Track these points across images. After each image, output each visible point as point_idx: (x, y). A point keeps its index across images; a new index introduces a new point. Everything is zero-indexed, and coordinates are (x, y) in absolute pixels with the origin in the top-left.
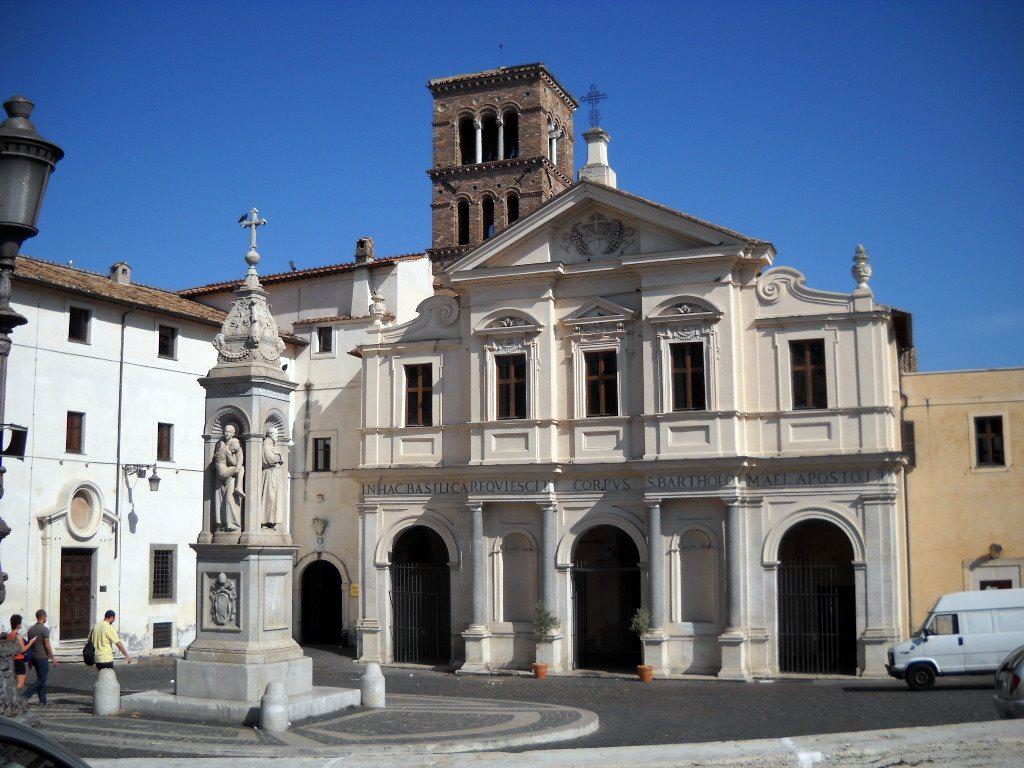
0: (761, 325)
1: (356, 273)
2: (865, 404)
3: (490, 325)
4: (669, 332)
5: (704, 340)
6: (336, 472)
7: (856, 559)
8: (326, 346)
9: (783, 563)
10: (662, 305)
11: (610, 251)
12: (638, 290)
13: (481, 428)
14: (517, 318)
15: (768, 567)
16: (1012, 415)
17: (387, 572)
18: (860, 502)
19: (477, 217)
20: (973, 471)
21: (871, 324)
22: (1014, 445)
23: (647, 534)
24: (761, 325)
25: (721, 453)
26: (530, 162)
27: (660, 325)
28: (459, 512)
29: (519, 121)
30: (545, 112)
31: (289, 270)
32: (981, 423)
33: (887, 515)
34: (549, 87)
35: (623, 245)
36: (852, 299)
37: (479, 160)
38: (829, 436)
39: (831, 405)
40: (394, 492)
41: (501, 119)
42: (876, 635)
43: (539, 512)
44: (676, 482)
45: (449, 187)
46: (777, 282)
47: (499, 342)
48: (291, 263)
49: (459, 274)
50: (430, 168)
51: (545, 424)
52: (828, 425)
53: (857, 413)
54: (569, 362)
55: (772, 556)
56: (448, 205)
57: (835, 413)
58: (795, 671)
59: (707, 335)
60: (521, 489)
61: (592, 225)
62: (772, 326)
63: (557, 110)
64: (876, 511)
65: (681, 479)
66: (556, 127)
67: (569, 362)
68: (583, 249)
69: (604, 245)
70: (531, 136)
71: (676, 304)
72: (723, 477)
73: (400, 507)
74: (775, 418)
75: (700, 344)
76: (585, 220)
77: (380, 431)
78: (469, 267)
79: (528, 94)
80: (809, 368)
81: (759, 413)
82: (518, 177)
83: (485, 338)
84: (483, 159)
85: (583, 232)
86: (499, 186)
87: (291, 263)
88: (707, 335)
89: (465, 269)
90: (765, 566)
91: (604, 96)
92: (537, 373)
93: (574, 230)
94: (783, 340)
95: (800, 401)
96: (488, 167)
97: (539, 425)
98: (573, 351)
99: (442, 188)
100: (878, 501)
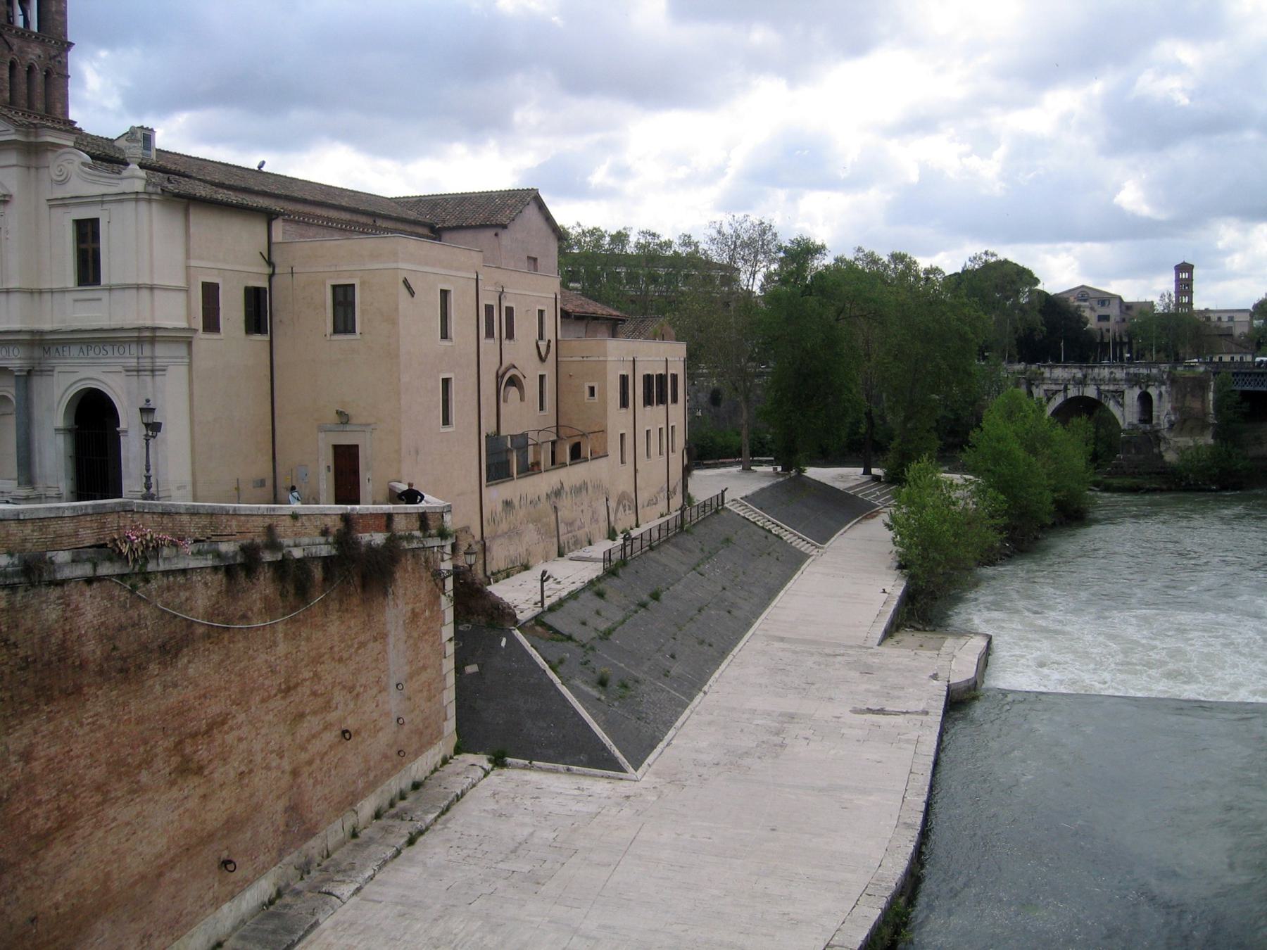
39: (103, 281)
90: (56, 430)
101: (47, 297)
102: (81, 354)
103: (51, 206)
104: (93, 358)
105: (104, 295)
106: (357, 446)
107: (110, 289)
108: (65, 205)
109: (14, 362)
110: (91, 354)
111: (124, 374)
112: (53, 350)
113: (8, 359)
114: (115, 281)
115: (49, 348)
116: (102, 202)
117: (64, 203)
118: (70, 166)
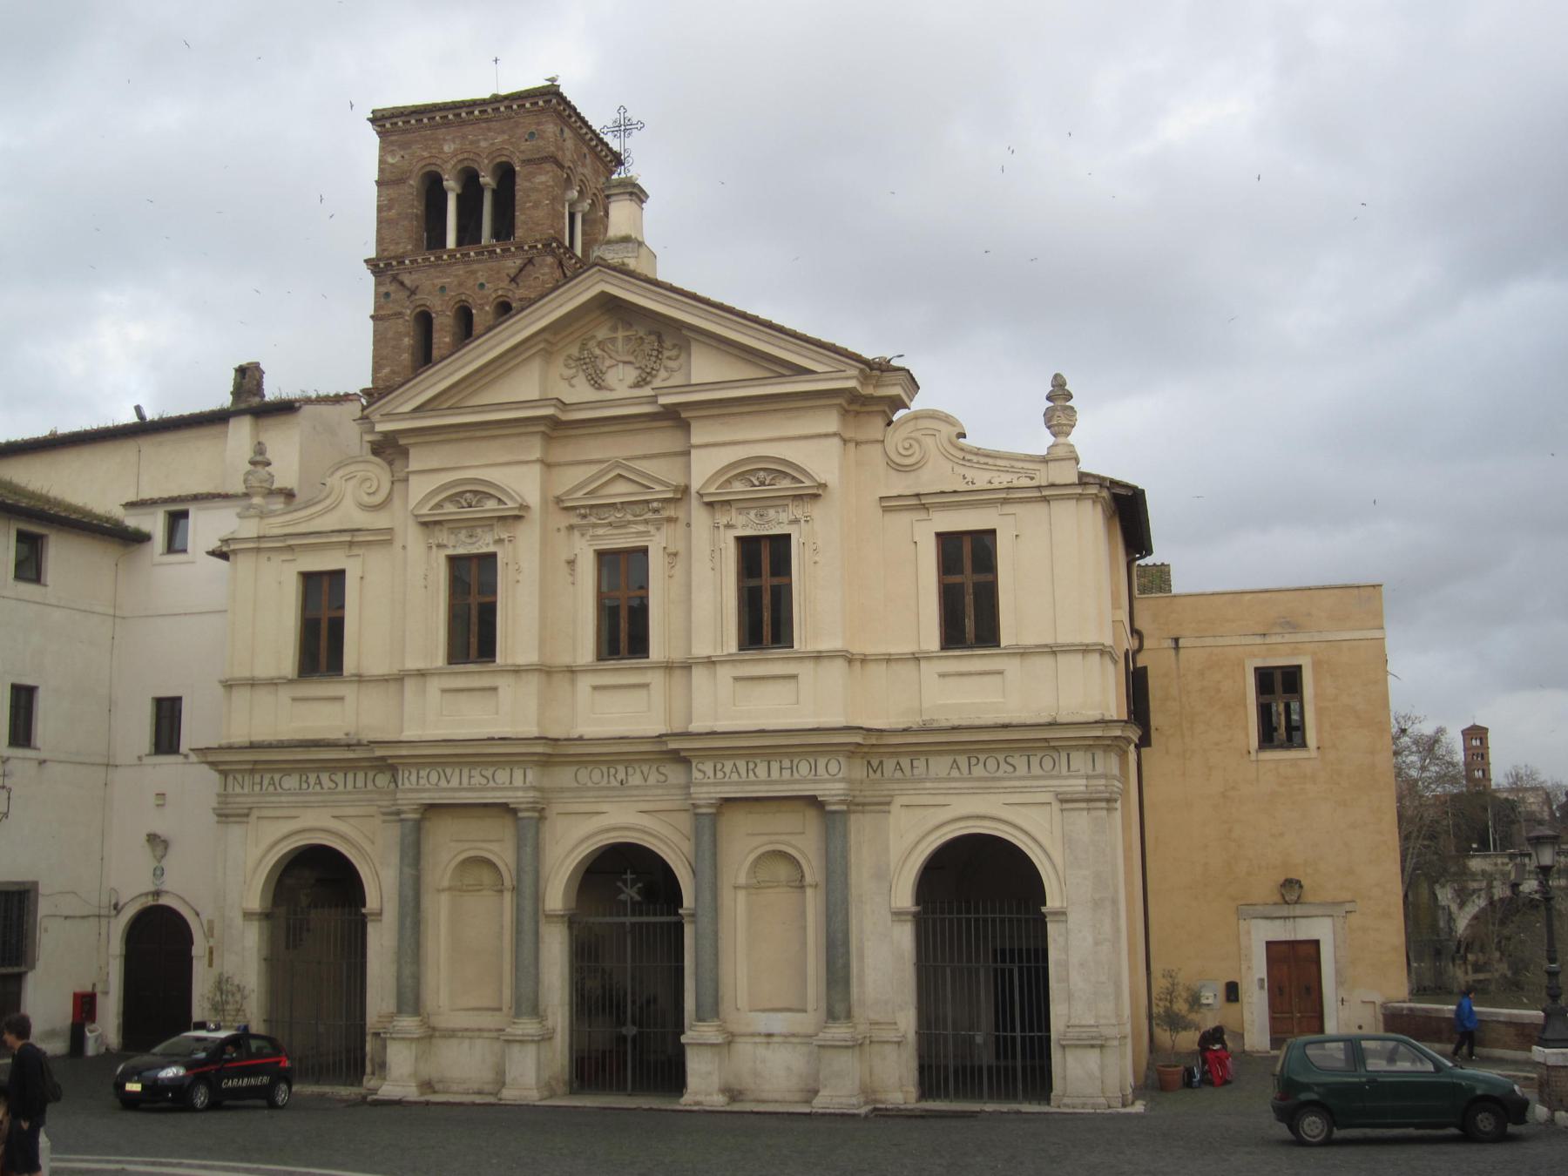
0: (889, 505)
1: (233, 423)
3: (439, 505)
8: (174, 544)
15: (898, 915)
16: (1317, 665)
19: (442, 338)
20: (1253, 756)
22: (1320, 712)
24: (889, 505)
28: (384, 822)
29: (518, 180)
30: (561, 166)
31: (132, 418)
32: (1265, 678)
34: (570, 127)
35: (663, 374)
37: (451, 241)
39: (1006, 638)
41: (487, 179)
42: (1084, 1035)
44: (743, 770)
48: (138, 409)
49: (389, 416)
50: (373, 255)
54: (571, 563)
55: (904, 896)
56: (399, 315)
58: (947, 1096)
60: (484, 781)
63: (584, 165)
65: (751, 766)
66: (581, 192)
69: (631, 374)
70: (536, 205)
71: (745, 471)
73: (285, 813)
78: (407, 408)
79: (532, 135)
80: (967, 578)
84: (460, 241)
85: (597, 352)
86: (482, 286)
87: (138, 409)
89: (401, 410)
91: (641, 125)
95: (953, 636)
99: (392, 288)
101: (875, 670)
102: (955, 773)
103: (886, 510)
104: (979, 779)
105: (1012, 666)
106: (1269, 944)
107: (1024, 653)
108: (924, 507)
109: (828, 786)
110: (978, 771)
111: (1056, 806)
112: (890, 764)
113: (815, 782)
114: (1030, 640)
115: (881, 763)
116: (1005, 501)
117: (920, 503)
118: (929, 441)
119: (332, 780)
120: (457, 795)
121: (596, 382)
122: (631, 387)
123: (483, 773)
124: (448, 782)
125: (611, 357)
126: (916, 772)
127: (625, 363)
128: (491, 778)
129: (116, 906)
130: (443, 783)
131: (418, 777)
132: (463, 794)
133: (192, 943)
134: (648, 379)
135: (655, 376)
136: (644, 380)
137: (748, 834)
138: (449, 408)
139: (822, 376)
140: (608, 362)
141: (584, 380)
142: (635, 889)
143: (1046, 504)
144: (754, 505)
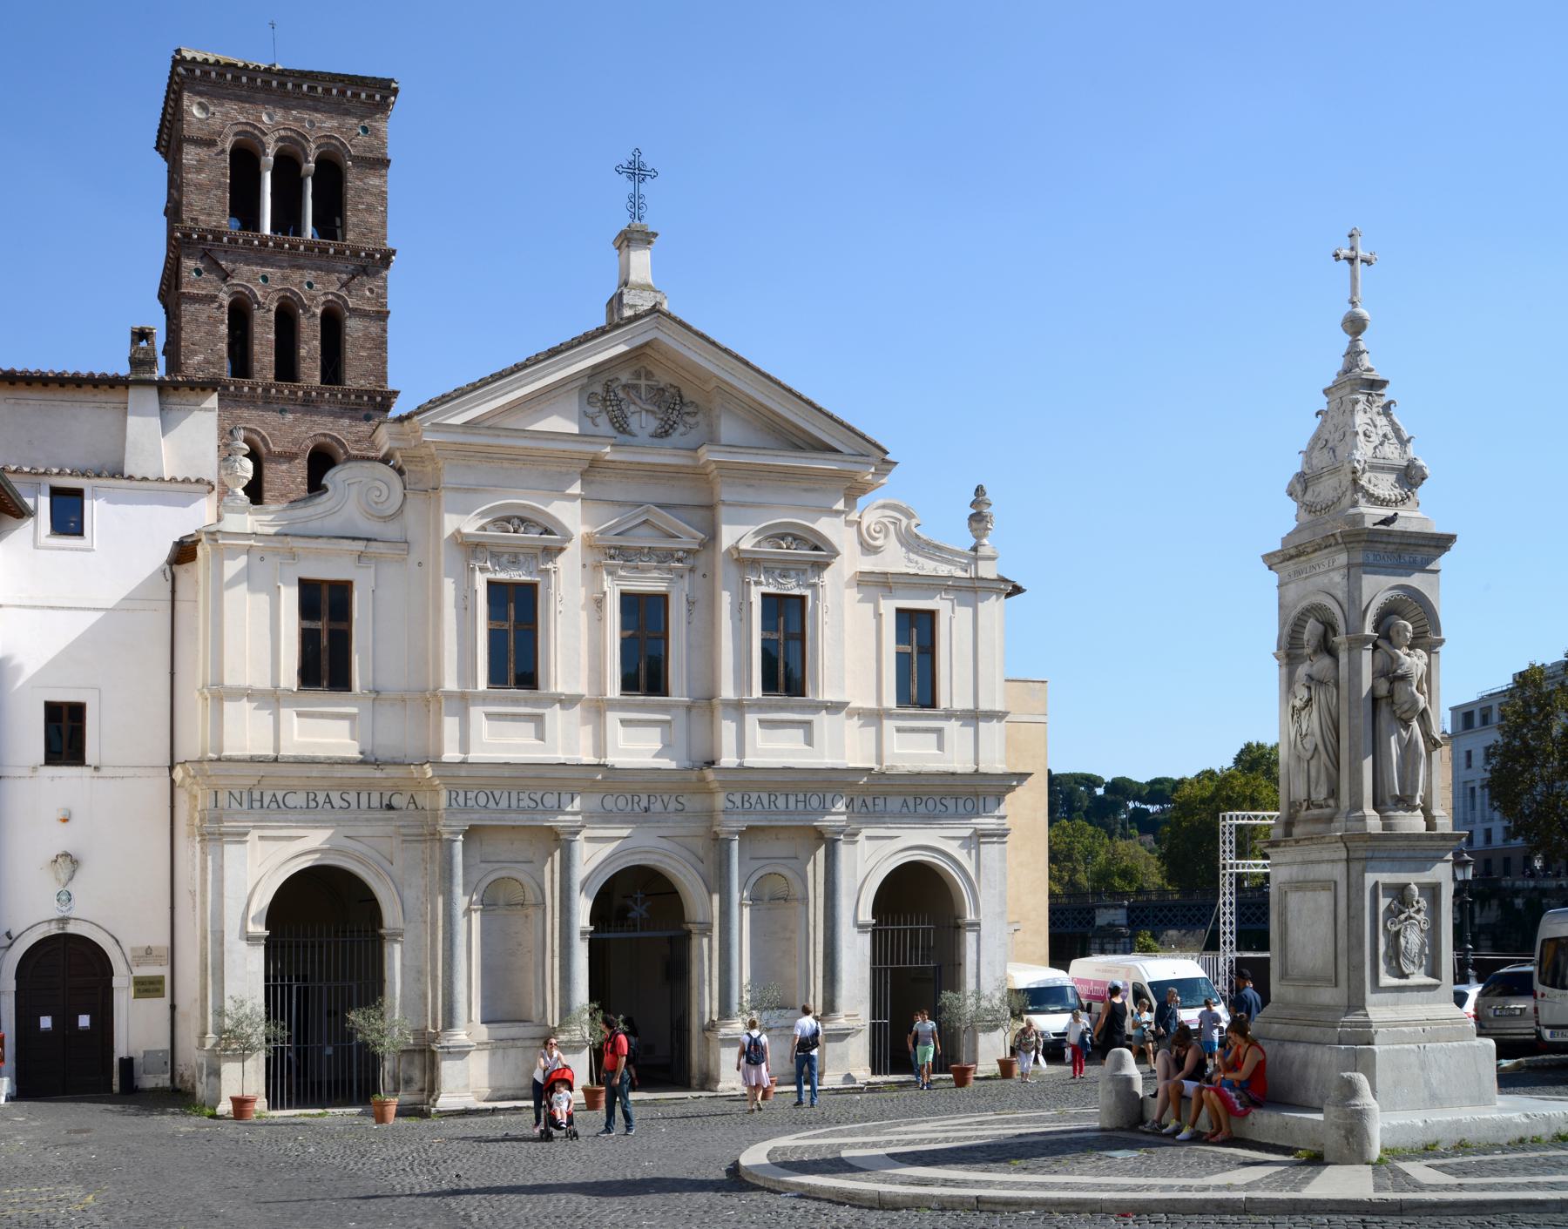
2: (984, 706)
4: (762, 576)
5: (808, 592)
6: (96, 768)
7: (968, 917)
9: (879, 923)
10: (757, 533)
11: (664, 433)
12: (711, 508)
13: (463, 701)
14: (524, 521)
17: (259, 952)
18: (980, 837)
21: (994, 597)
23: (720, 883)
25: (827, 761)
26: (370, 255)
27: (747, 562)
33: (1003, 859)
35: (681, 429)
36: (976, 559)
38: (940, 747)
40: (281, 806)
43: (560, 841)
45: (214, 266)
46: (885, 520)
47: (495, 556)
51: (567, 702)
52: (939, 731)
53: (974, 717)
57: (950, 715)
59: (814, 586)
60: (533, 805)
61: (636, 387)
62: (877, 584)
64: (989, 851)
67: (599, 603)
68: (621, 426)
69: (652, 424)
72: (829, 797)
74: (874, 717)
75: (802, 598)
76: (625, 377)
77: (250, 694)
78: (458, 420)
81: (859, 709)
82: (344, 277)
83: (471, 548)
85: (621, 395)
88: (814, 586)
92: (559, 616)
93: (608, 390)
94: (889, 607)
96: (279, 245)
97: (560, 701)
98: (606, 589)
100: (995, 839)
119: (344, 800)
120: (507, 816)
121: (621, 426)
122: (652, 436)
123: (532, 796)
124: (497, 804)
125: (634, 403)
126: (877, 808)
127: (647, 411)
128: (539, 801)
129: (8, 935)
130: (492, 804)
131: (466, 799)
132: (513, 815)
133: (112, 974)
134: (671, 431)
135: (675, 430)
136: (666, 432)
137: (752, 859)
138: (489, 428)
139: (846, 458)
140: (632, 408)
141: (607, 420)
142: (644, 907)
143: (972, 594)
144: (780, 565)
